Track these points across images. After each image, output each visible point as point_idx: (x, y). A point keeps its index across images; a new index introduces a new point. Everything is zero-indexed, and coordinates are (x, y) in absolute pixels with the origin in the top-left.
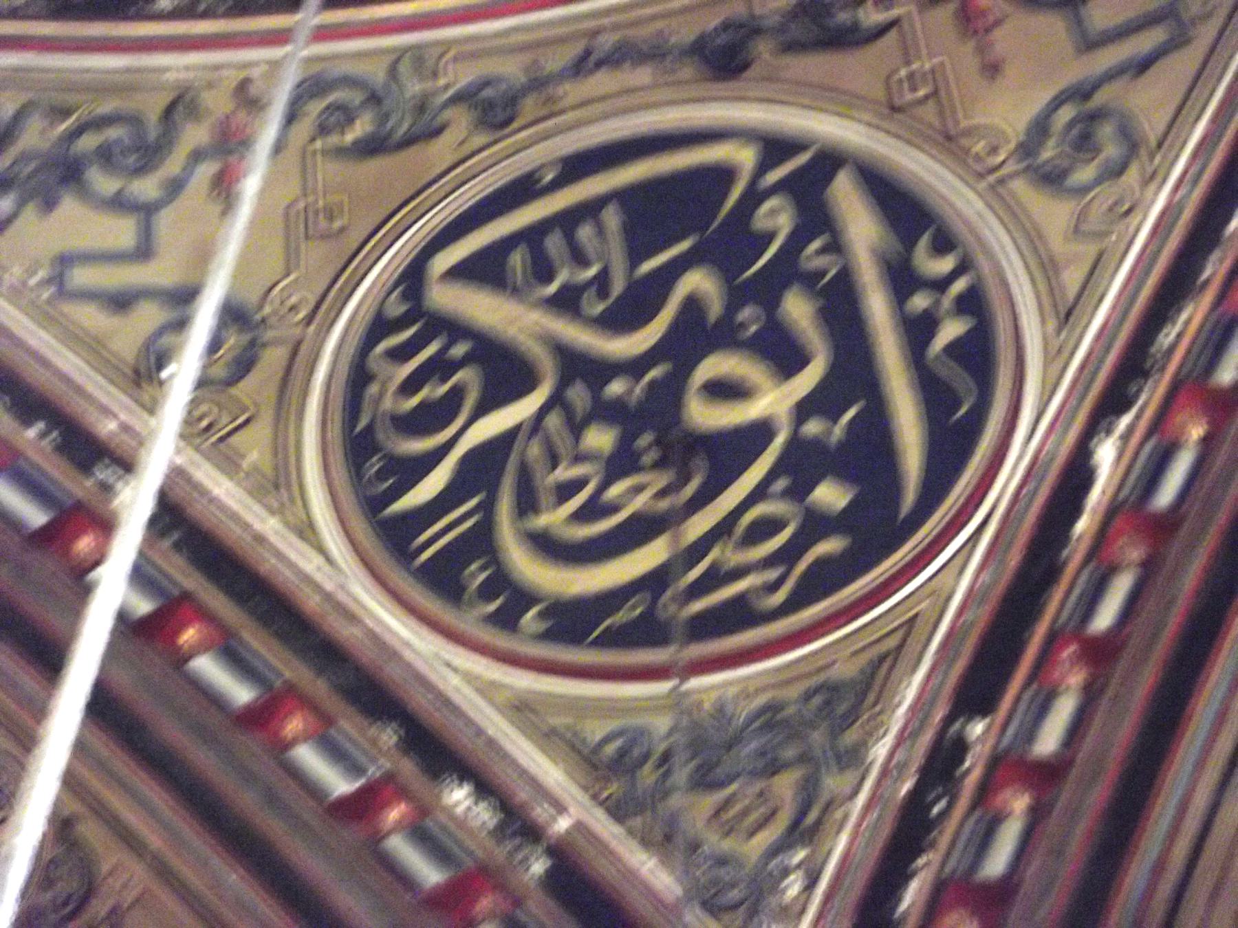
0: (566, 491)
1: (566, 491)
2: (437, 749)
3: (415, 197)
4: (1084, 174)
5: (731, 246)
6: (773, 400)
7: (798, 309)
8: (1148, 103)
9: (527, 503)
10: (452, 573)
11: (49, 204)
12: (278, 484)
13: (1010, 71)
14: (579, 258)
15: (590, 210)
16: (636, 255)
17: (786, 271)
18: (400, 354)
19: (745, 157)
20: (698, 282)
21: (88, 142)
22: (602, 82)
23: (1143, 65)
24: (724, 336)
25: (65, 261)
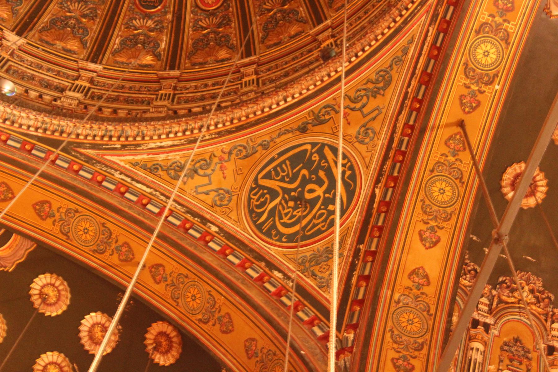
0: (286, 215)
1: (286, 215)
2: (271, 266)
3: (255, 165)
4: (367, 140)
5: (308, 165)
6: (320, 191)
7: (321, 174)
8: (376, 125)
9: (281, 218)
10: (269, 232)
11: (192, 178)
12: (238, 221)
13: (352, 124)
14: (283, 171)
15: (284, 162)
16: (293, 168)
17: (319, 167)
18: (255, 194)
19: (309, 147)
20: (304, 172)
21: (198, 165)
22: (283, 137)
23: (374, 119)
24: (310, 181)
25: (196, 188)
